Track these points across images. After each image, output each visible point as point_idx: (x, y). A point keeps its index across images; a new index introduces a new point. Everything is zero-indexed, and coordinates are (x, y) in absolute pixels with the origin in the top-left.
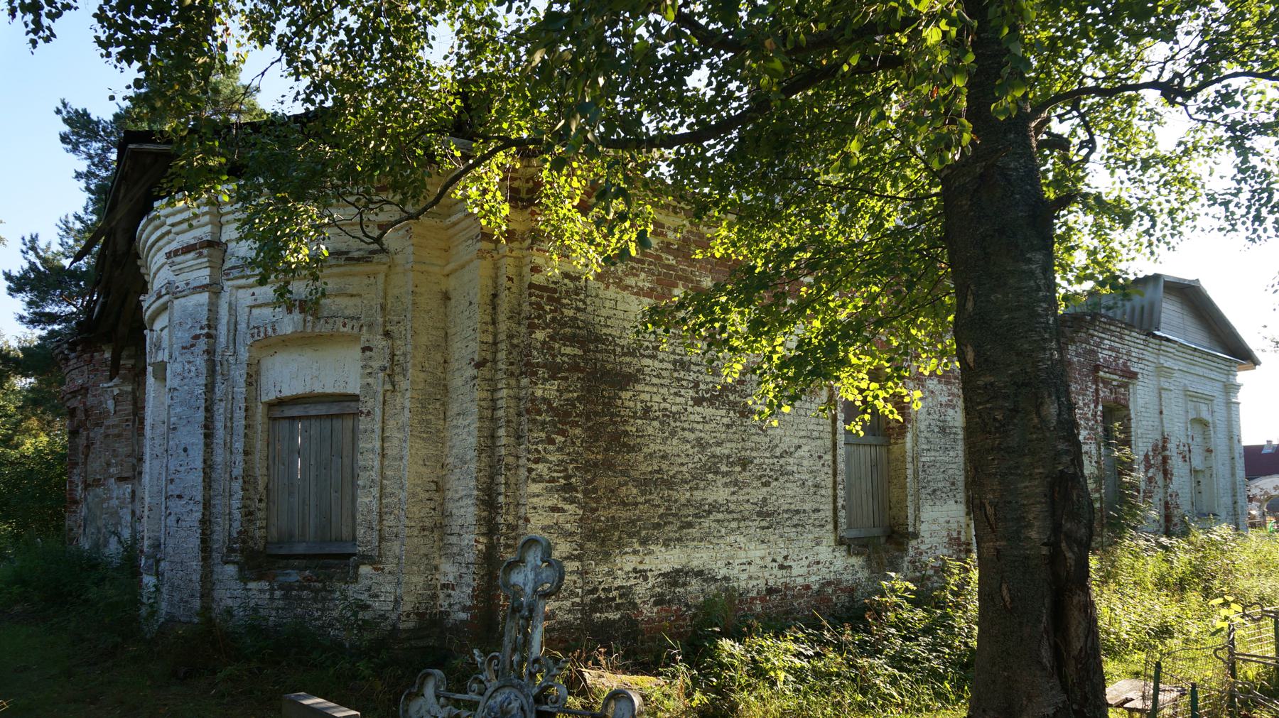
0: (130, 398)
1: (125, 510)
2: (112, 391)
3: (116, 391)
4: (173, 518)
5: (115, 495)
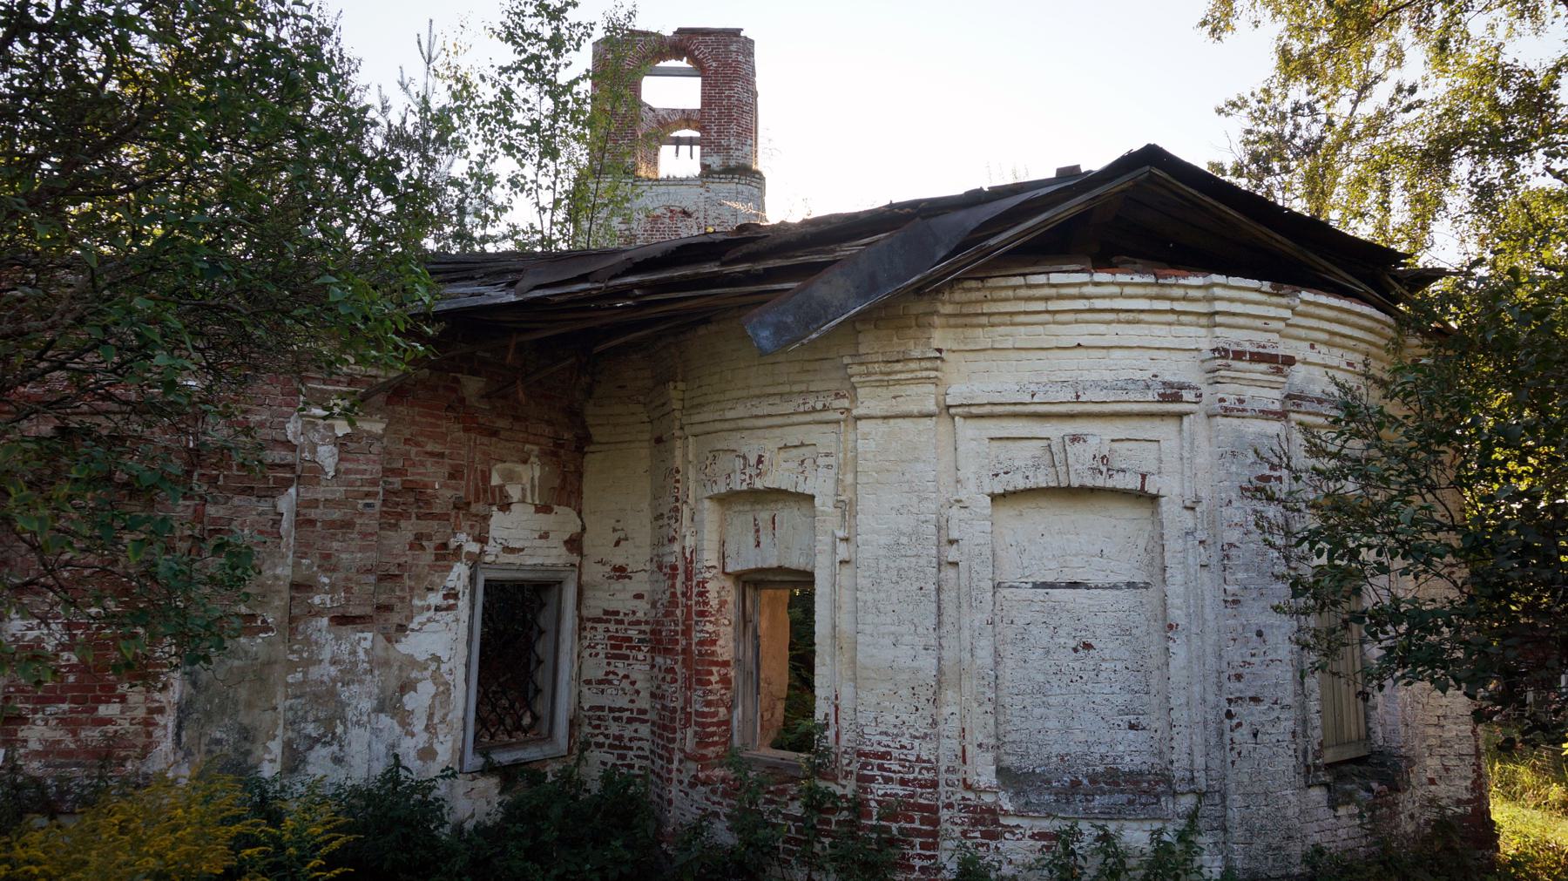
1: (355, 688)
2: (332, 428)
4: (1245, 730)
5: (326, 654)
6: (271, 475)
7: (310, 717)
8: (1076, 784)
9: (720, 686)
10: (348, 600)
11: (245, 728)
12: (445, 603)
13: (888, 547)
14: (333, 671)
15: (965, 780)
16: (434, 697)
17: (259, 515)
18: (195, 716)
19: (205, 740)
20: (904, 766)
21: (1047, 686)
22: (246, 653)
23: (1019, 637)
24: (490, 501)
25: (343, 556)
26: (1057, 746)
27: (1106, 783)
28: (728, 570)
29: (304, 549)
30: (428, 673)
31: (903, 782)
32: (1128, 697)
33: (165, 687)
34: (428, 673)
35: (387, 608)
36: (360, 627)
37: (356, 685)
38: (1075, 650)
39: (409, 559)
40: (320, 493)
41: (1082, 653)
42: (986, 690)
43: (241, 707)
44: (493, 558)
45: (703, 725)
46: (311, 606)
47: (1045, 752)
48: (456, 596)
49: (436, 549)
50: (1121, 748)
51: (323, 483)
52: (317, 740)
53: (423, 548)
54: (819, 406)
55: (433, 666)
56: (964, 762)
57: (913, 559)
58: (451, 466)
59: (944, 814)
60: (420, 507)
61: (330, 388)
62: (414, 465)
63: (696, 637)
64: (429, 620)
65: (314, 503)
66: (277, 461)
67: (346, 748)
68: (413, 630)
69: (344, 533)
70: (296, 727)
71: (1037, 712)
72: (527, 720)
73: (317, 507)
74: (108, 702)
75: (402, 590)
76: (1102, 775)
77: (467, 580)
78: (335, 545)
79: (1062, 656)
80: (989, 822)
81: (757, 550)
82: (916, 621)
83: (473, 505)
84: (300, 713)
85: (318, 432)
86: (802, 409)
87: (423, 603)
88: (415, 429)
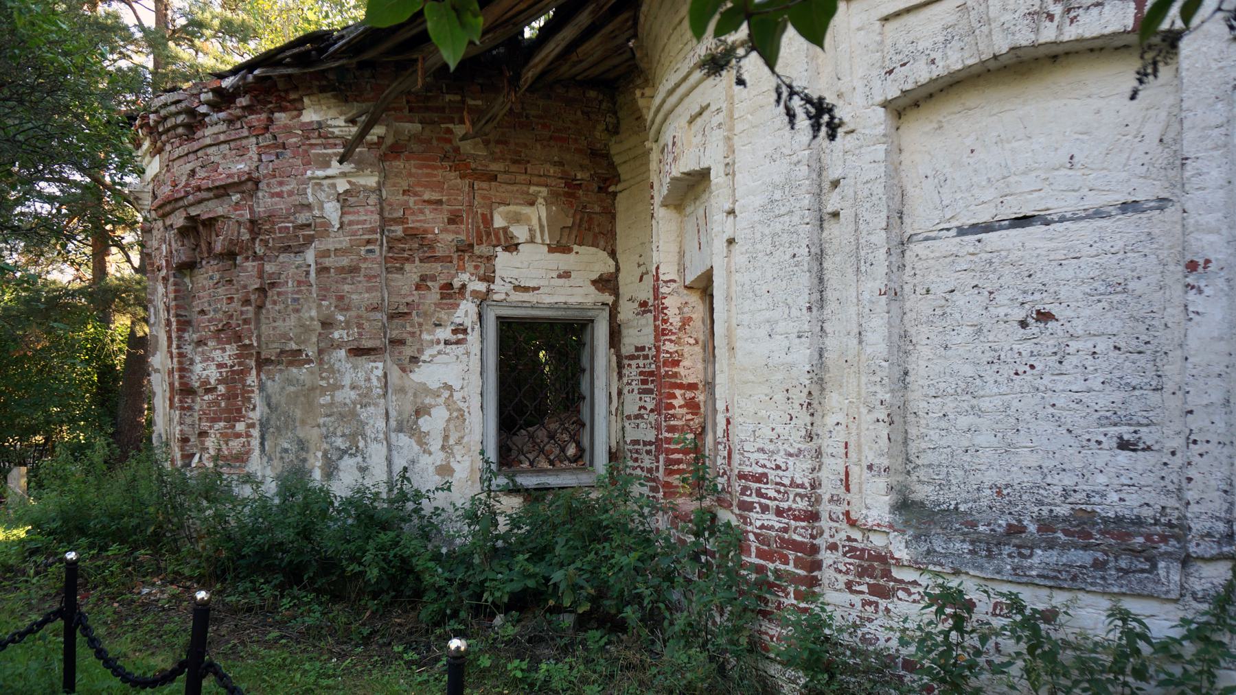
0: (373, 199)
1: (371, 409)
2: (334, 186)
3: (342, 186)
5: (347, 381)
6: (301, 233)
7: (339, 433)
8: (1015, 530)
9: (684, 410)
10: (360, 334)
11: (301, 441)
12: (454, 338)
13: (763, 209)
14: (353, 395)
15: (847, 514)
16: (449, 420)
17: (297, 268)
18: (271, 430)
19: (278, 449)
20: (779, 492)
21: (978, 381)
22: (298, 380)
23: (940, 312)
24: (494, 242)
25: (354, 297)
26: (992, 473)
27: (1066, 533)
28: (687, 283)
29: (324, 293)
30: (441, 400)
31: (779, 512)
32: (1118, 396)
33: (254, 409)
34: (441, 400)
35: (398, 342)
36: (372, 358)
37: (372, 408)
38: (1023, 324)
39: (416, 298)
40: (330, 244)
41: (1034, 328)
42: (878, 388)
43: (297, 424)
44: (503, 296)
45: (668, 452)
46: (332, 340)
47: (973, 481)
48: (465, 331)
49: (441, 288)
50: (1101, 479)
51: (332, 235)
52: (345, 452)
53: (428, 288)
55: (446, 394)
56: (848, 489)
57: (787, 218)
58: (448, 211)
59: (827, 557)
60: (425, 252)
61: (330, 151)
62: (413, 213)
64: (439, 353)
65: (325, 254)
66: (304, 222)
67: (368, 460)
68: (424, 362)
69: (353, 277)
70: (329, 440)
71: (964, 422)
72: (571, 450)
73: (329, 256)
74: (239, 421)
75: (412, 326)
76: (1065, 519)
77: (475, 317)
78: (347, 288)
79: (1001, 336)
80: (878, 572)
82: (790, 301)
83: (476, 247)
84: (331, 429)
85: (324, 191)
87: (432, 337)
88: (412, 180)
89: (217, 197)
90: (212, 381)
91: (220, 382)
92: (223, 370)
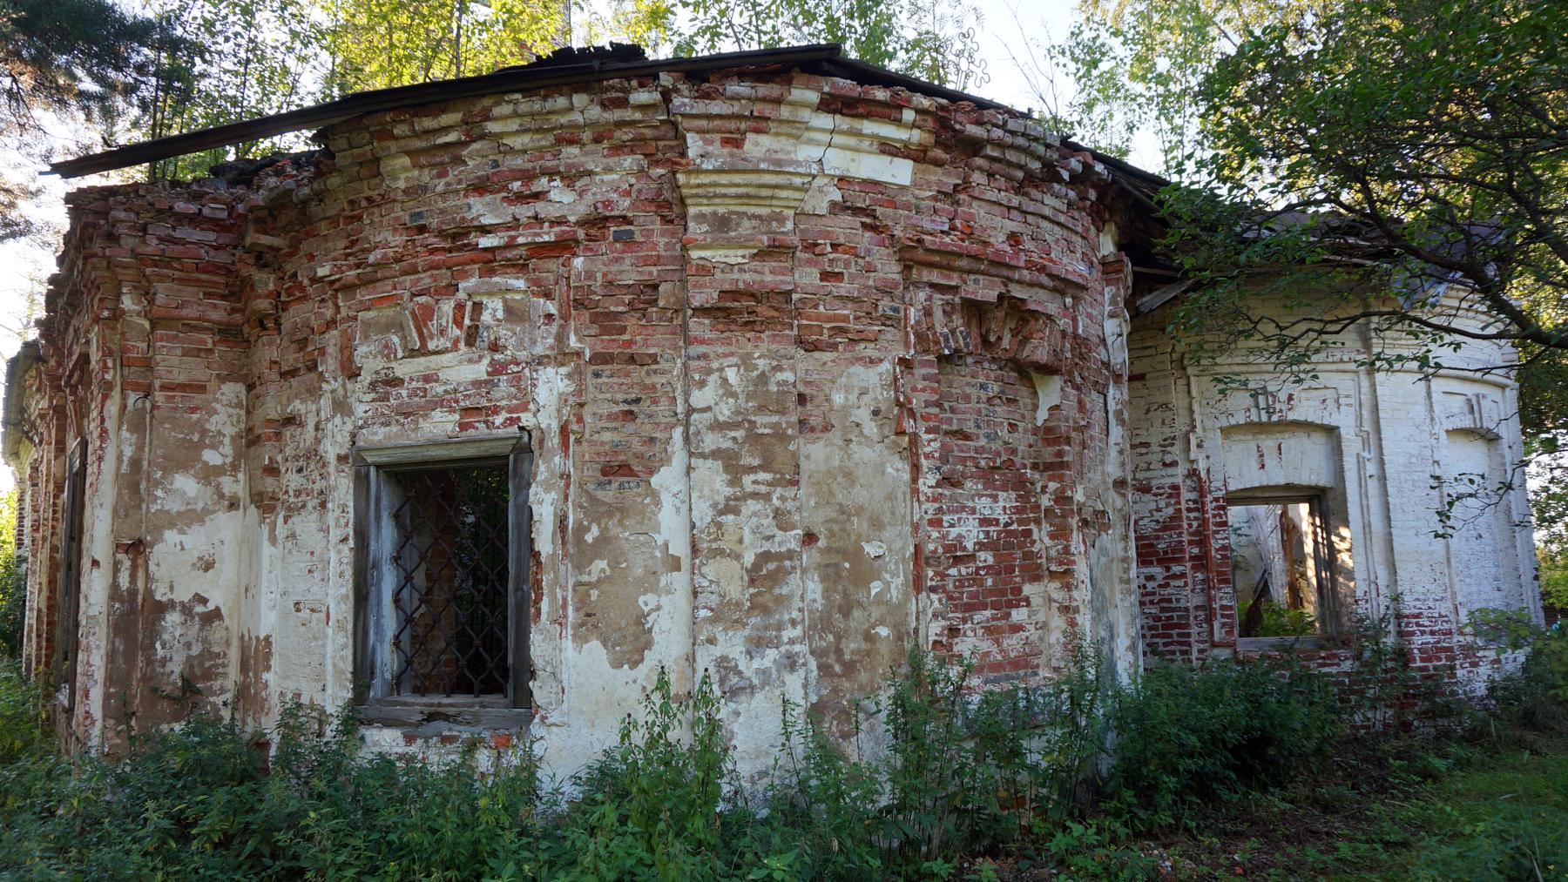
31: (1432, 633)
54: (1346, 358)
63: (1215, 544)
74: (1018, 606)
81: (1262, 471)
86: (1330, 359)
89: (1054, 290)
90: (970, 546)
91: (981, 546)
92: (992, 528)
